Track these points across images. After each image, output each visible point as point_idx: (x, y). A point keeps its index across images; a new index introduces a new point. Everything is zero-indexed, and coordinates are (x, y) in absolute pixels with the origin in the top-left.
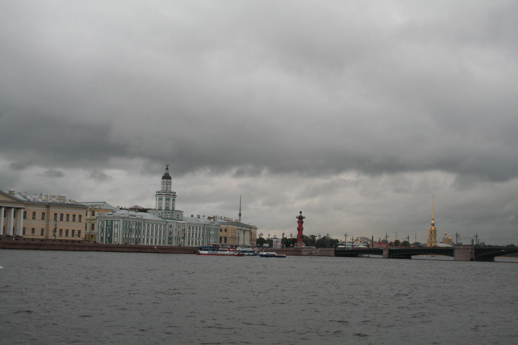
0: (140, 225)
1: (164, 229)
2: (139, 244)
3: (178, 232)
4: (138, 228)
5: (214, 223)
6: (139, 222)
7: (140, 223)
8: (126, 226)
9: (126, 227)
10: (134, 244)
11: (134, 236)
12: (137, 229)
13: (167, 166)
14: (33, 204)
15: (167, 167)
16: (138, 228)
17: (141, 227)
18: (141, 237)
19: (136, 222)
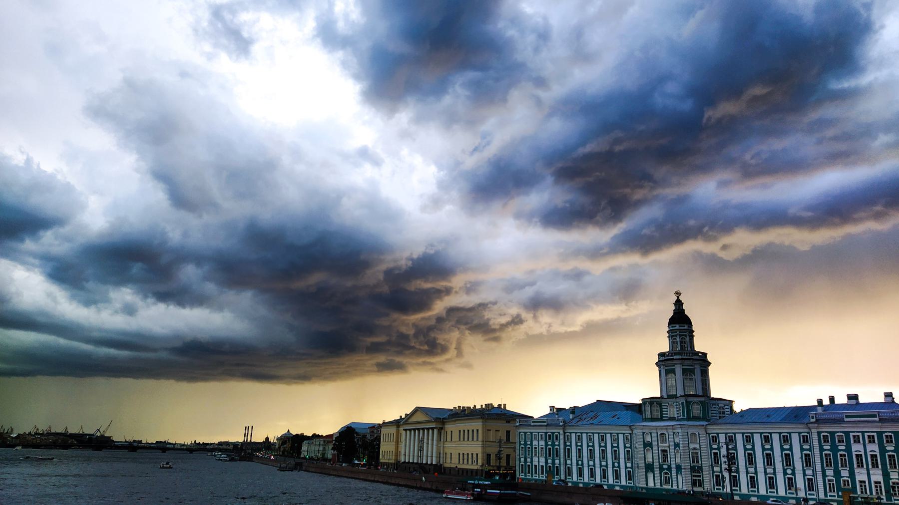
0: (557, 439)
1: (628, 445)
3: (664, 451)
5: (875, 416)
6: (553, 433)
8: (525, 441)
9: (525, 444)
10: (544, 478)
11: (542, 463)
13: (678, 294)
15: (678, 297)
16: (553, 445)
17: (559, 442)
18: (560, 464)
19: (546, 433)
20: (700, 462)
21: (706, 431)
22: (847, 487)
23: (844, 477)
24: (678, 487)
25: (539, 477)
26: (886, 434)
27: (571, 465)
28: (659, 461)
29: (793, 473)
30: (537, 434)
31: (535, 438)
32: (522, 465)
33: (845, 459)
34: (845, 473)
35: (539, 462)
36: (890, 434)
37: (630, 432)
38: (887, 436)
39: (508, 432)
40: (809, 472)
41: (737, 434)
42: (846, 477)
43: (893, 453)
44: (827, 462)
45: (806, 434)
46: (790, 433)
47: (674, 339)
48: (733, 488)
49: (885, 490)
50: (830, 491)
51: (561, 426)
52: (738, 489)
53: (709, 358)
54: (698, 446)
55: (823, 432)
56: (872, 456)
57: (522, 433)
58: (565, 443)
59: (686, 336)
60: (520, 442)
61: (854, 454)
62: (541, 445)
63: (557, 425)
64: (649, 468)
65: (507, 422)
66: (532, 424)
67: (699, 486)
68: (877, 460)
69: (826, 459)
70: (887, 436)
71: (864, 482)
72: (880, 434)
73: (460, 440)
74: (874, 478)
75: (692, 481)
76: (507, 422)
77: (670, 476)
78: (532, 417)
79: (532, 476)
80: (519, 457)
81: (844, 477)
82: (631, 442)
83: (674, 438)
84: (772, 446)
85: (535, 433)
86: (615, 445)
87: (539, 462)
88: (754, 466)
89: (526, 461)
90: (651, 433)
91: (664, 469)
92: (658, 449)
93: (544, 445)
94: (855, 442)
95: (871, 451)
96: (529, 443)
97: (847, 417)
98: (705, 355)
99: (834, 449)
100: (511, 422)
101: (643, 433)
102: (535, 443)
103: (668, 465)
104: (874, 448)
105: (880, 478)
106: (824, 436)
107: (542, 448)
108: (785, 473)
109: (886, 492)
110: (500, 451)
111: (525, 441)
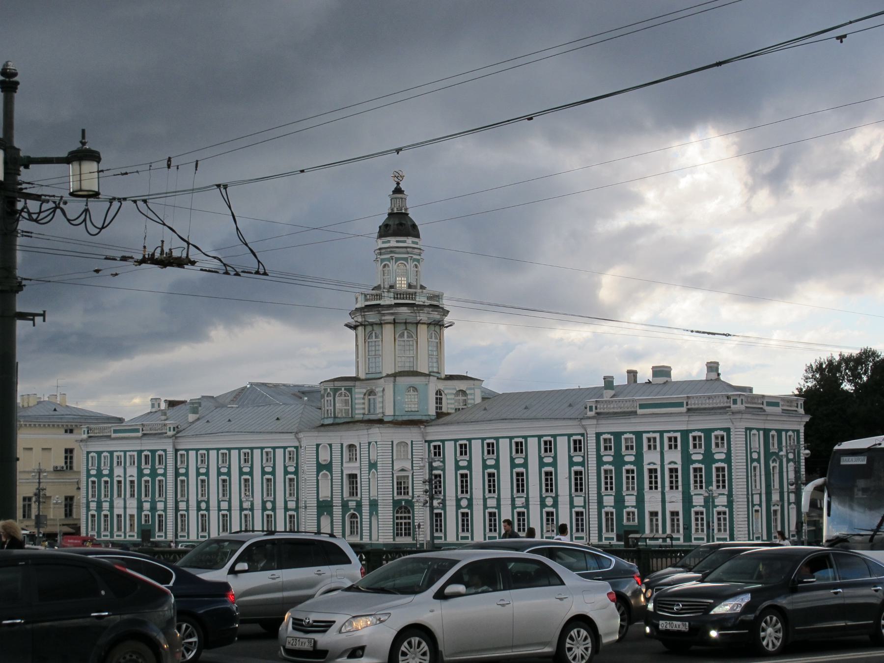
1: (291, 469)
2: (157, 539)
3: (353, 477)
4: (154, 474)
5: (680, 405)
6: (153, 452)
7: (160, 456)
8: (99, 470)
9: (99, 474)
10: (135, 538)
11: (132, 509)
13: (398, 177)
14: (49, 425)
15: (398, 184)
16: (154, 474)
17: (165, 469)
18: (165, 510)
19: (140, 452)
20: (410, 494)
21: (423, 437)
22: (631, 523)
23: (628, 507)
24: (371, 539)
25: (125, 537)
26: (694, 434)
27: (187, 510)
28: (342, 495)
29: (555, 504)
30: (122, 454)
31: (119, 463)
32: (93, 516)
33: (633, 478)
34: (630, 500)
35: (125, 508)
36: (699, 434)
37: (297, 444)
38: (694, 438)
39: (69, 452)
40: (579, 501)
41: (473, 441)
42: (633, 507)
43: (700, 465)
44: (606, 483)
45: (579, 437)
46: (554, 436)
47: (385, 266)
48: (436, 535)
49: (684, 525)
50: (607, 531)
51: (170, 437)
52: (442, 535)
53: (446, 304)
54: (408, 465)
55: (604, 433)
56: (671, 470)
57: (92, 454)
58: (177, 469)
59: (406, 259)
60: (88, 471)
61: (646, 468)
62: (130, 476)
63: (160, 435)
64: (324, 507)
65: (66, 431)
66: (113, 435)
67: (405, 535)
68: (677, 477)
69: (606, 478)
70: (694, 438)
71: (656, 514)
72: (685, 433)
74: (669, 508)
75: (394, 527)
76: (66, 431)
77: (359, 520)
78: (120, 420)
79: (112, 536)
80: (87, 500)
81: (628, 507)
82: (297, 464)
83: (369, 453)
84: (526, 459)
85: (118, 454)
87: (125, 508)
88: (496, 495)
89: (99, 508)
90: (330, 445)
91: (349, 510)
93: (136, 475)
94: (649, 447)
95: (670, 463)
96: (106, 472)
97: (642, 406)
99: (619, 461)
100: (75, 431)
101: (318, 446)
102: (118, 471)
103: (356, 501)
104: (674, 457)
105: (679, 507)
106: (605, 440)
107: (132, 482)
108: (543, 505)
109: (684, 528)
110: (39, 489)
111: (99, 470)
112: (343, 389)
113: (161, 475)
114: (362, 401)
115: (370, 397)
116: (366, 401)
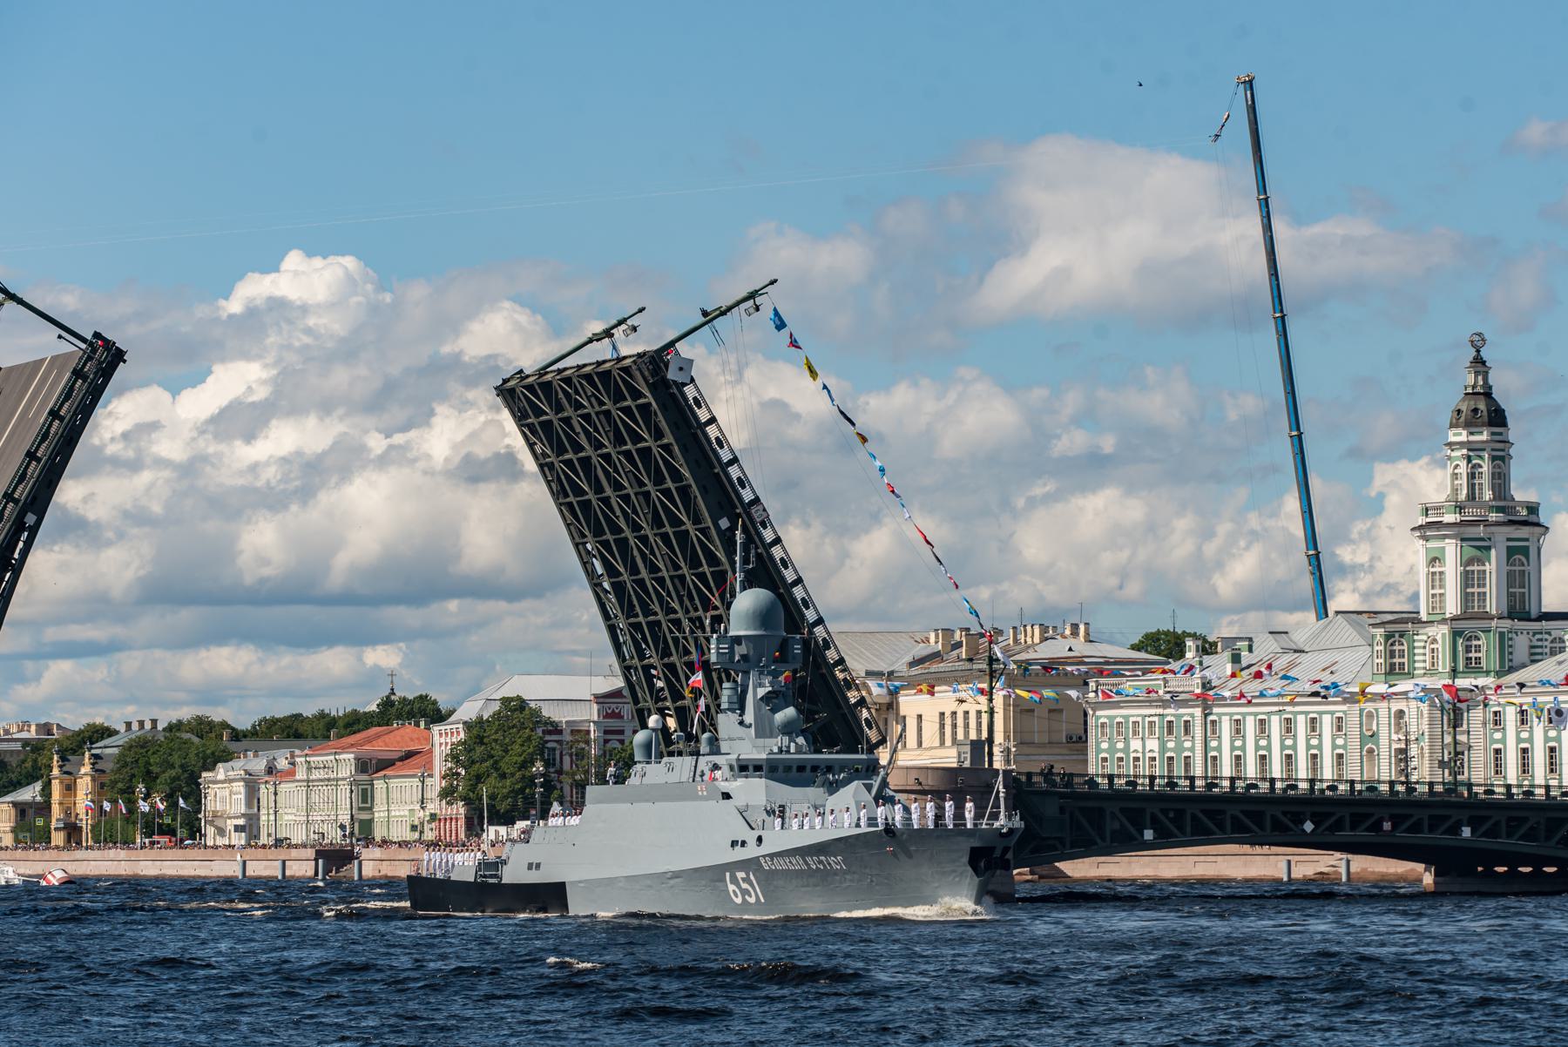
0: (1187, 731)
4: (1179, 748)
12: (1169, 754)
13: (1478, 342)
15: (1478, 351)
16: (1179, 748)
62: (1150, 751)
73: (942, 742)
86: (1314, 742)
92: (1390, 748)
93: (1157, 750)
98: (1533, 509)
102: (1135, 744)
107: (1154, 759)
112: (1397, 635)
113: (1188, 749)
114: (1421, 651)
115: (1432, 646)
116: (1427, 651)
